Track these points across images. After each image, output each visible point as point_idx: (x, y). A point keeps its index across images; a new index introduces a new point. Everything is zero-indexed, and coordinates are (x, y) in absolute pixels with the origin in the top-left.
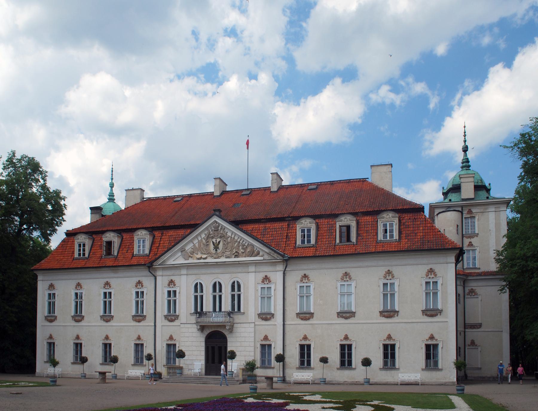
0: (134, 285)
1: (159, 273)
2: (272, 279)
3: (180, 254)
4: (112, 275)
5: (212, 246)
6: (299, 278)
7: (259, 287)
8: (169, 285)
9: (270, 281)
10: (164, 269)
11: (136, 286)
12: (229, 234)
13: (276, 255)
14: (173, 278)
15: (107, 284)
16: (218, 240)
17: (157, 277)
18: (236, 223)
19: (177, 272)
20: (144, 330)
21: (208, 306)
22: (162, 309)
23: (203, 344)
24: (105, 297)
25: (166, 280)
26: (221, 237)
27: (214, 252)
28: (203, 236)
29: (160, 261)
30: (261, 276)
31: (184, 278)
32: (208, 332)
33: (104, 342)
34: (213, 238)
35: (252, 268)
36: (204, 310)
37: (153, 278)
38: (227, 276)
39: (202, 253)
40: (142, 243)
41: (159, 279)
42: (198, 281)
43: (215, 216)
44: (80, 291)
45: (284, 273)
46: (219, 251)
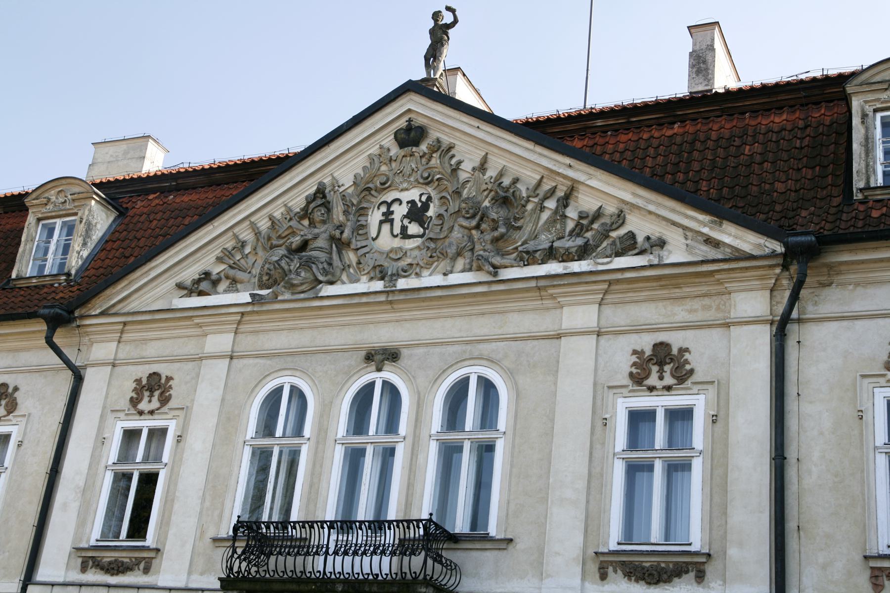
2: (695, 360)
7: (621, 408)
9: (683, 375)
12: (469, 161)
17: (90, 376)
35: (581, 314)
41: (94, 380)
42: (286, 381)
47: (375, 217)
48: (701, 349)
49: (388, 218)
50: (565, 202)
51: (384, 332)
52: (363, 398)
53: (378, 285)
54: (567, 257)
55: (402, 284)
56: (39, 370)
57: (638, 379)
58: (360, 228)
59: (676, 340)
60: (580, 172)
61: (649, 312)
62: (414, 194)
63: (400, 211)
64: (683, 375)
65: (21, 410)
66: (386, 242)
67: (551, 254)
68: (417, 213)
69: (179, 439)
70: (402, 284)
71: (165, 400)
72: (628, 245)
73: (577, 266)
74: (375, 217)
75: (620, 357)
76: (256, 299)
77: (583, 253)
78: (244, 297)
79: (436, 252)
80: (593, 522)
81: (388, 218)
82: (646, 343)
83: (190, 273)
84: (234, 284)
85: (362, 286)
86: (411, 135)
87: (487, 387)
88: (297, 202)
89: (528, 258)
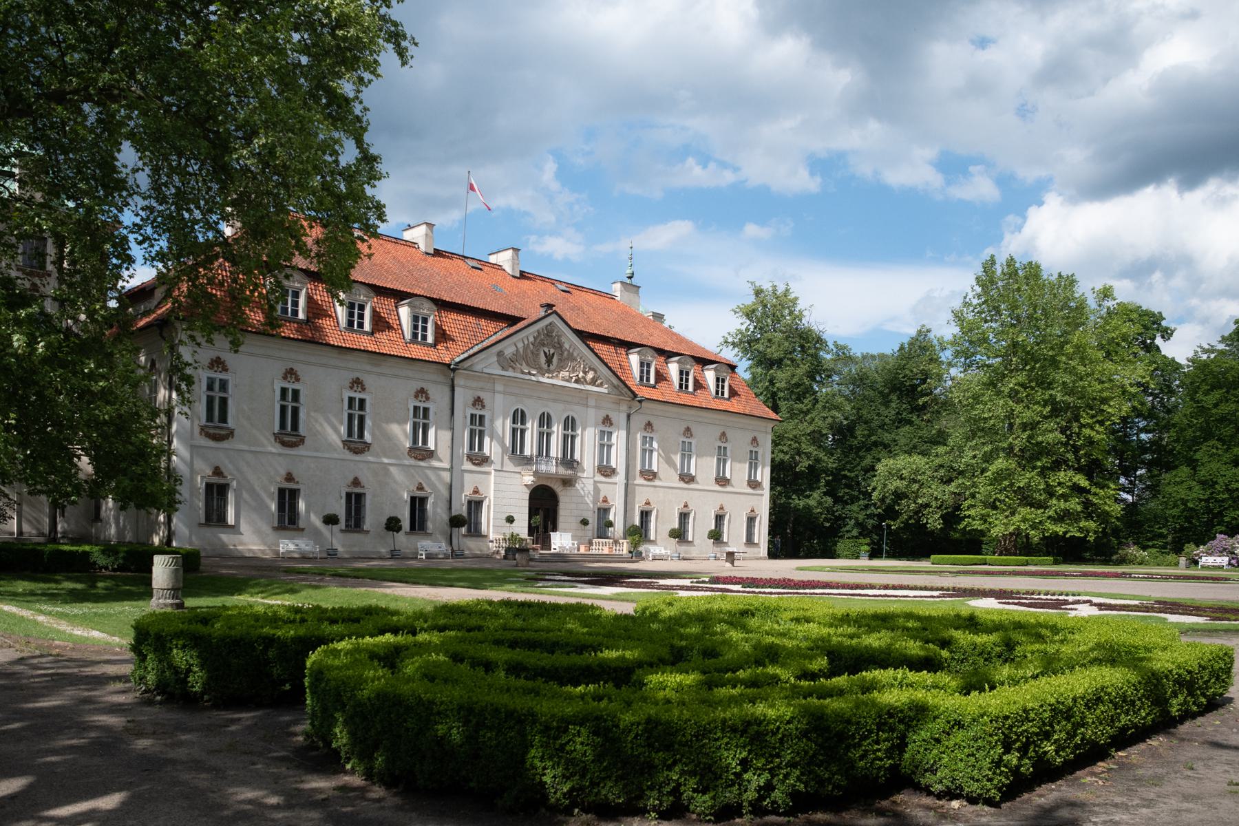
0: (413, 393)
2: (614, 420)
3: (495, 359)
4: (368, 368)
5: (543, 359)
6: (643, 426)
8: (474, 405)
10: (467, 377)
12: (567, 346)
14: (482, 395)
16: (552, 351)
18: (581, 334)
24: (350, 407)
26: (554, 347)
27: (545, 366)
28: (531, 339)
30: (603, 414)
33: (349, 490)
34: (543, 345)
36: (527, 452)
37: (447, 390)
38: (560, 406)
39: (528, 365)
42: (520, 407)
43: (554, 316)
44: (223, 376)
46: (552, 367)
56: (434, 382)
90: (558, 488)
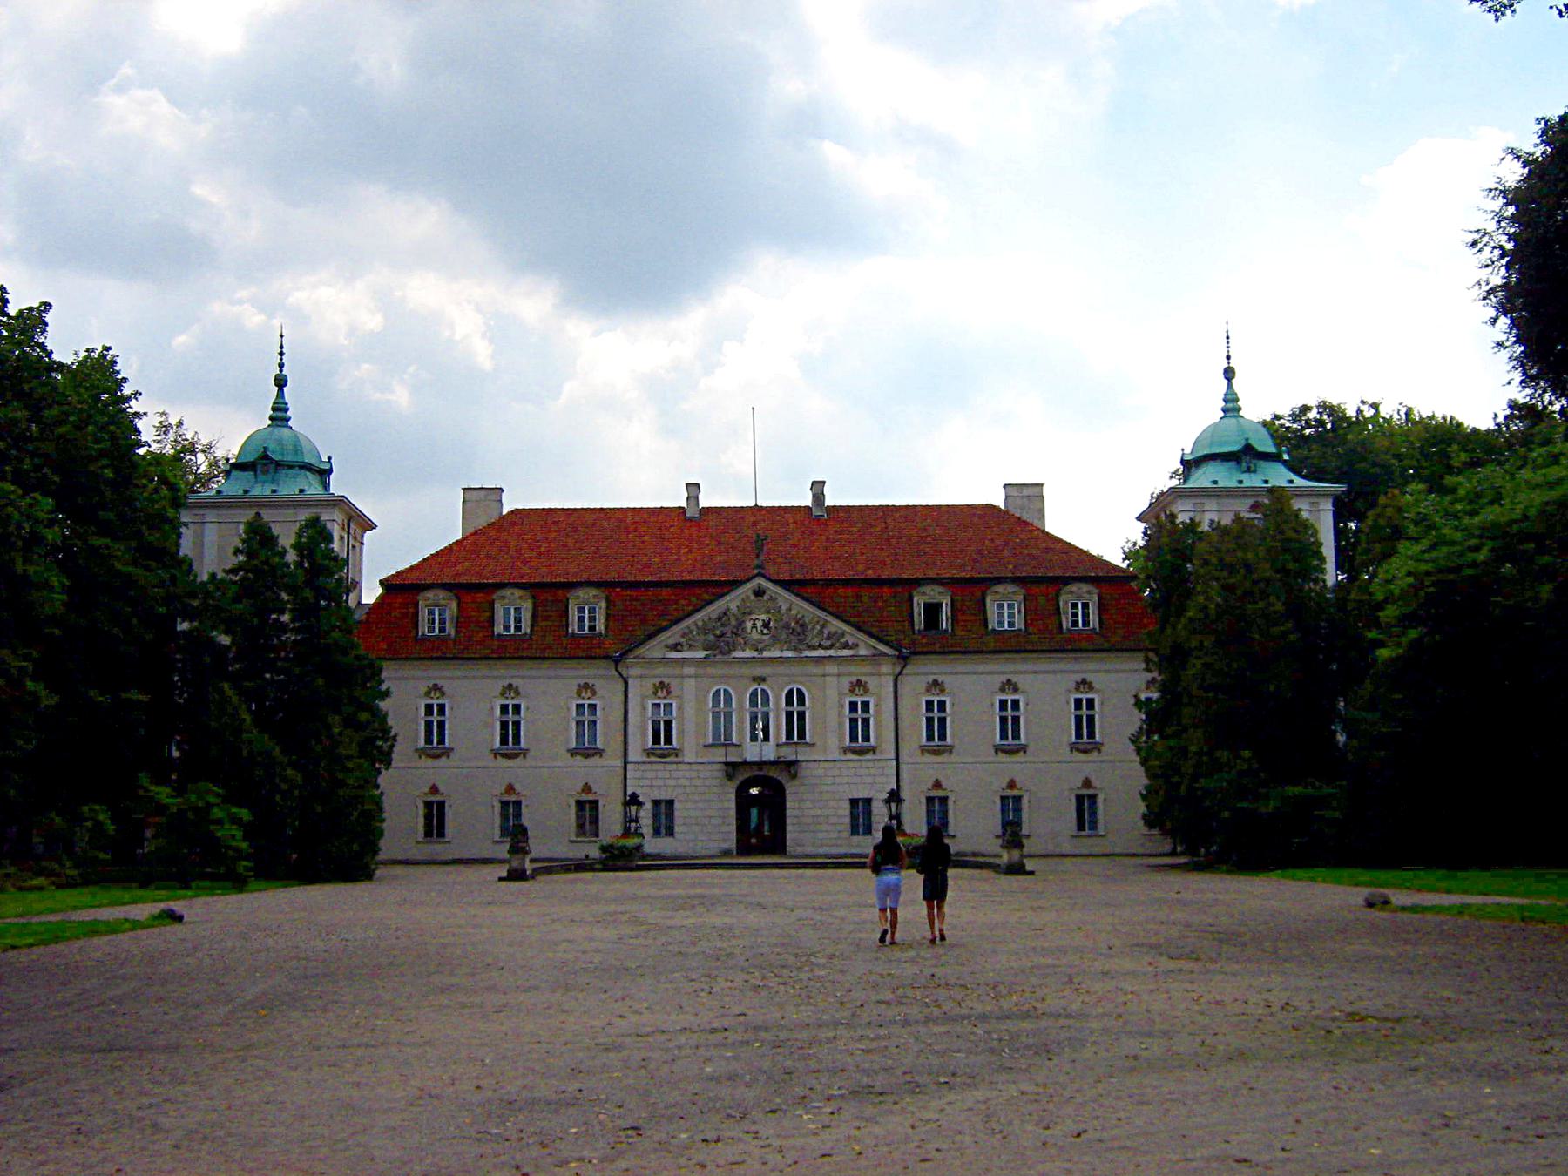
1: (633, 671)
9: (866, 691)
11: (579, 693)
13: (882, 648)
15: (509, 689)
17: (630, 681)
19: (677, 672)
20: (603, 777)
21: (740, 729)
22: (640, 739)
23: (733, 797)
25: (650, 683)
29: (639, 652)
31: (690, 684)
32: (746, 776)
35: (832, 669)
40: (588, 612)
42: (722, 687)
45: (896, 681)
47: (749, 625)
48: (872, 683)
49: (754, 626)
50: (823, 626)
51: (759, 671)
52: (754, 694)
53: (755, 654)
54: (826, 648)
55: (766, 654)
57: (852, 691)
58: (744, 630)
59: (863, 679)
60: (829, 618)
61: (852, 669)
62: (763, 617)
63: (759, 624)
64: (866, 691)
65: (599, 693)
66: (755, 635)
67: (820, 646)
68: (766, 625)
69: (679, 709)
70: (766, 654)
71: (669, 692)
72: (846, 646)
73: (831, 652)
74: (749, 625)
75: (846, 682)
76: (706, 657)
77: (831, 647)
78: (702, 654)
79: (775, 640)
80: (841, 740)
81: (754, 626)
82: (854, 679)
83: (671, 641)
84: (691, 647)
85: (748, 653)
86: (759, 593)
87: (801, 694)
88: (714, 616)
89: (813, 648)
90: (782, 777)
